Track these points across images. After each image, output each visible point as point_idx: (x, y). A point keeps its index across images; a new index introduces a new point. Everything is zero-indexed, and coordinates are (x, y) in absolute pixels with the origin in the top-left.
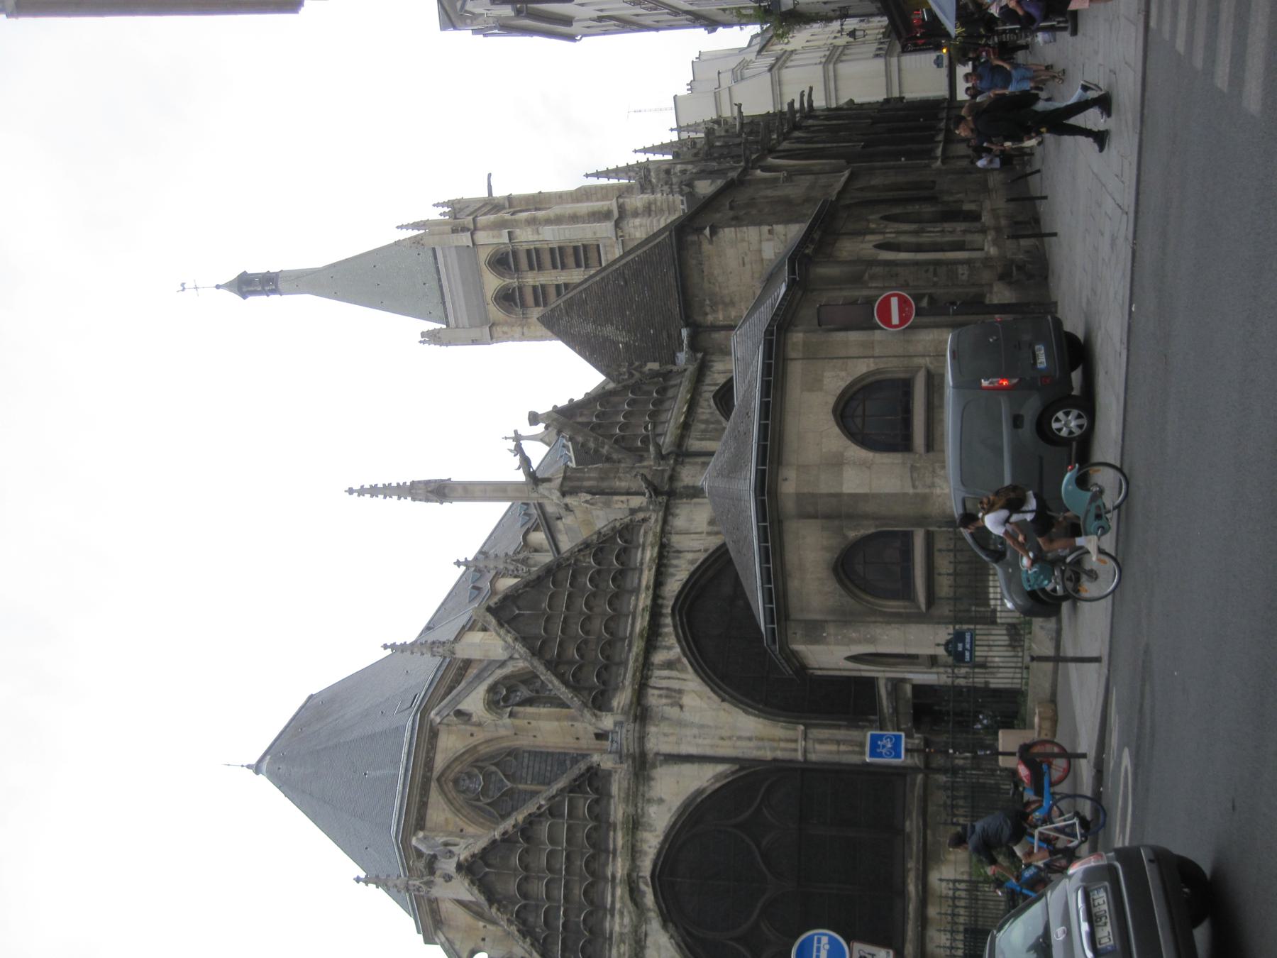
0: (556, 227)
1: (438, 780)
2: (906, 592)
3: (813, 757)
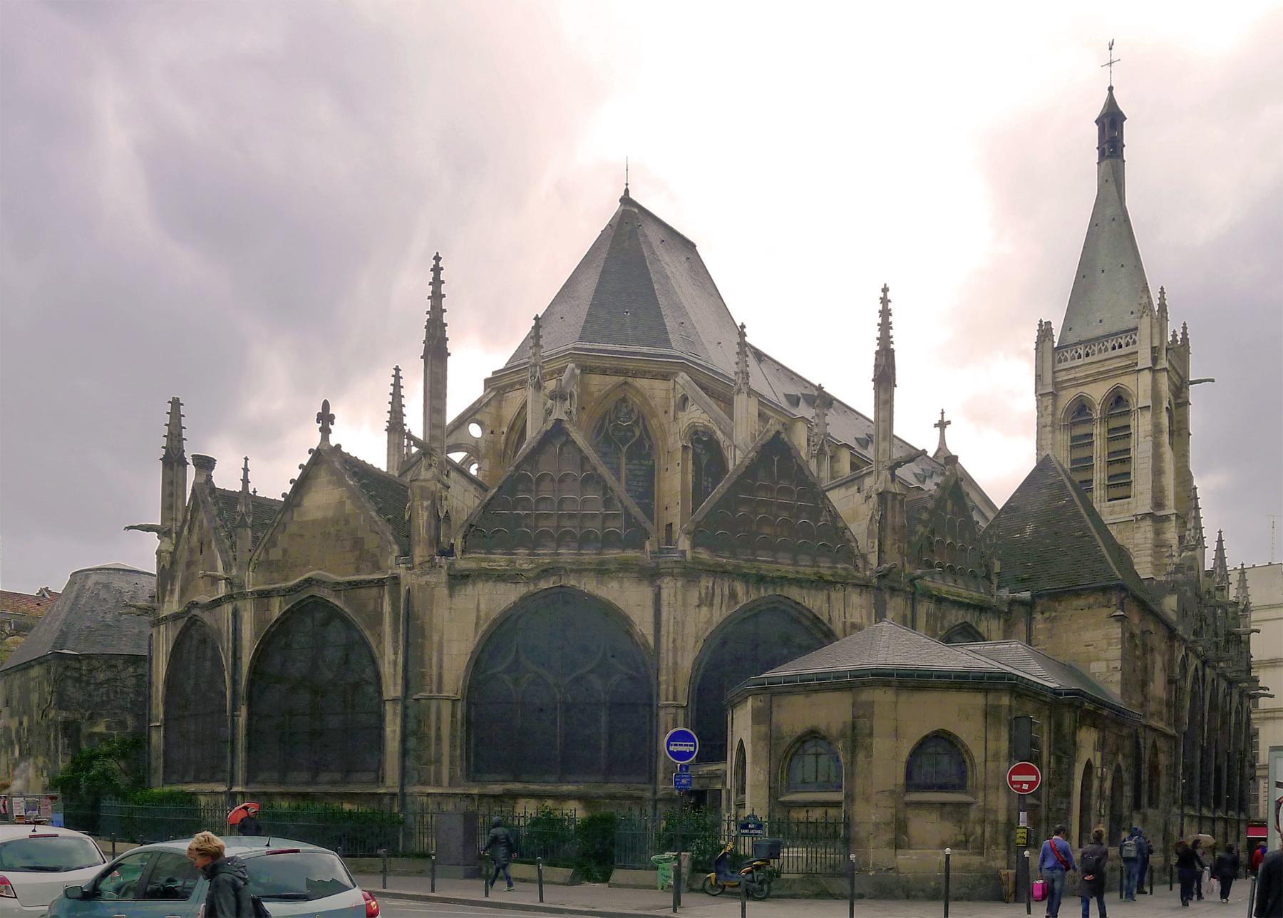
0: (1150, 454)
1: (626, 383)
3: (662, 713)
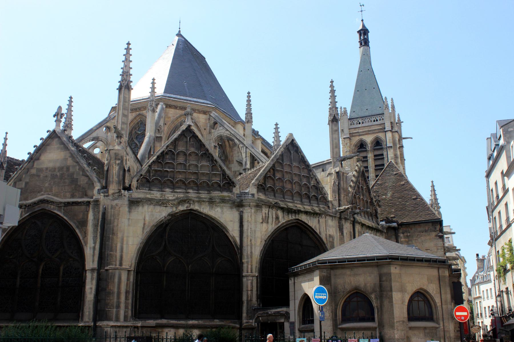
2: (345, 319)
3: (245, 280)
